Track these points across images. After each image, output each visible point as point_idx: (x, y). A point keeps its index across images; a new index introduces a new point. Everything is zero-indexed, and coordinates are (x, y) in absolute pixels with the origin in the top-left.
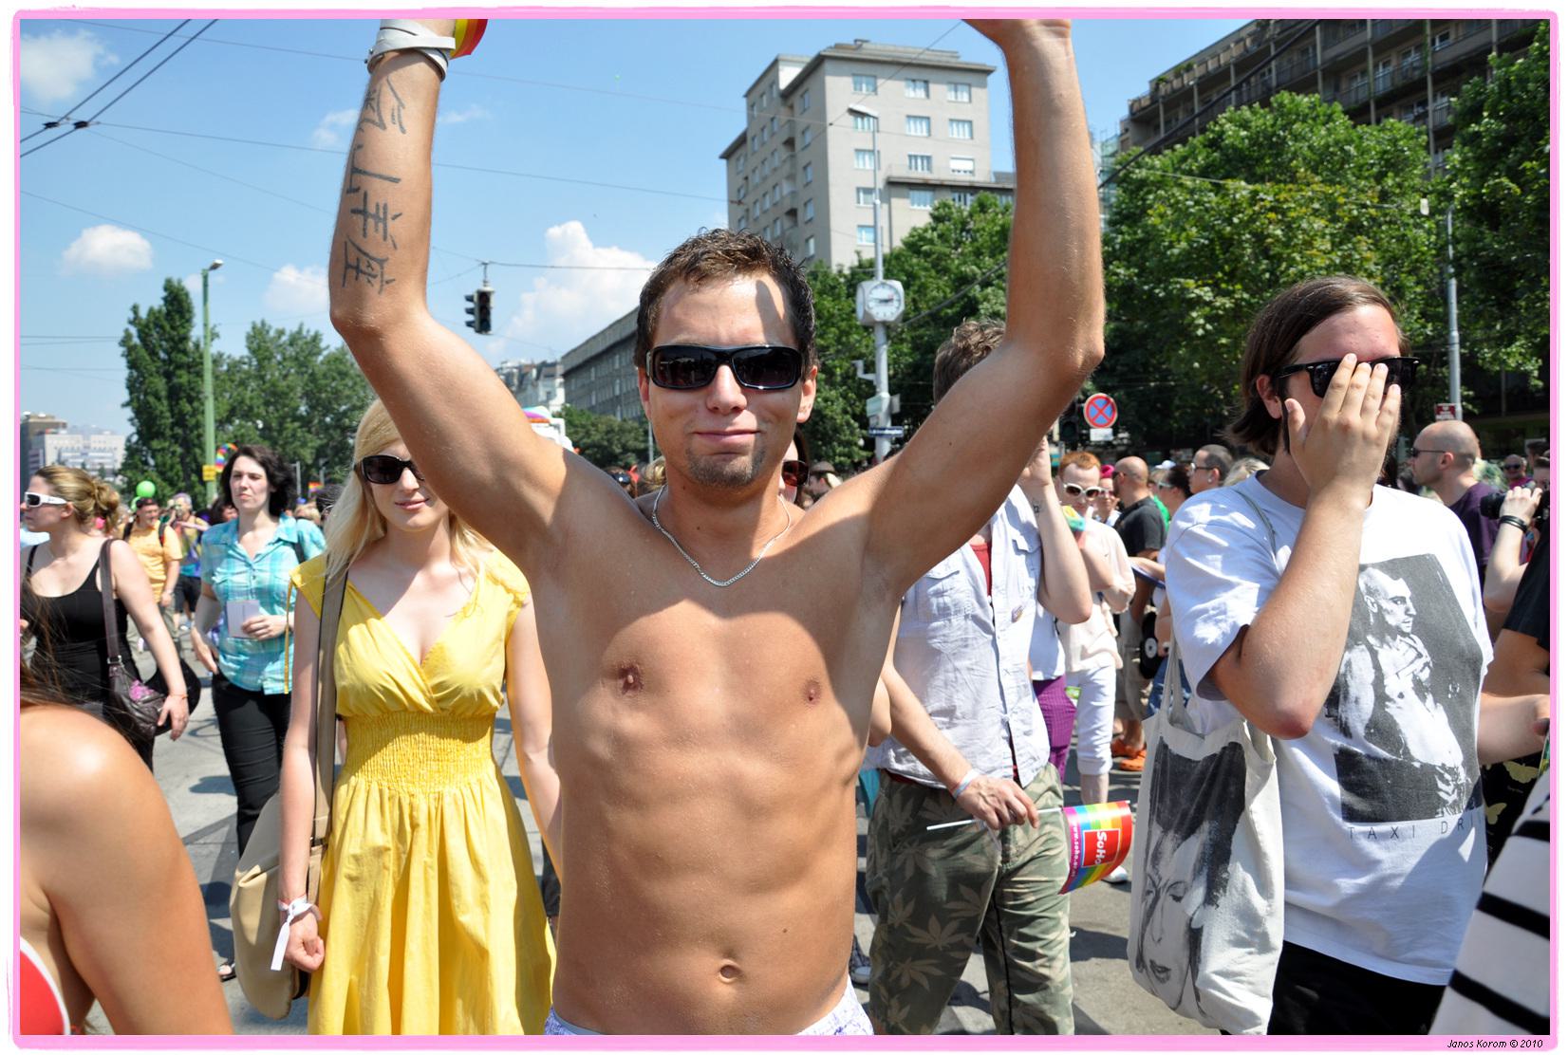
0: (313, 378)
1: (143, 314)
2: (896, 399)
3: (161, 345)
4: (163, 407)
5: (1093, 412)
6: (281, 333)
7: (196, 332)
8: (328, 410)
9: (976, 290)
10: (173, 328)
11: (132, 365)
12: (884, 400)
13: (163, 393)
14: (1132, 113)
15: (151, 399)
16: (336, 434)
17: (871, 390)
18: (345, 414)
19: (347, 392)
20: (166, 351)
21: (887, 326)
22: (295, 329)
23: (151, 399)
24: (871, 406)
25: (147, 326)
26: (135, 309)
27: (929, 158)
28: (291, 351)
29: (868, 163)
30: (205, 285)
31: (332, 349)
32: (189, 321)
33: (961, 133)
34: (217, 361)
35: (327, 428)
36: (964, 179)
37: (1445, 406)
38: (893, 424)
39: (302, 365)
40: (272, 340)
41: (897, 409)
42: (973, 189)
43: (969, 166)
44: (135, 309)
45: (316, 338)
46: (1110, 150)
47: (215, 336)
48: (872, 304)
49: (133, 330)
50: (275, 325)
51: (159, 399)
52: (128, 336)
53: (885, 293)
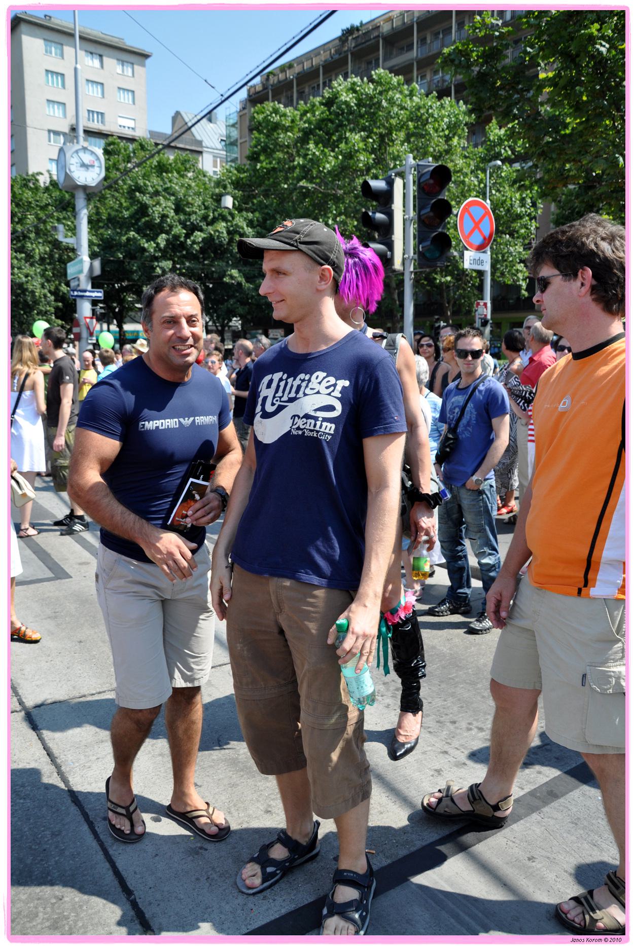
2: (97, 264)
5: (468, 225)
9: (146, 199)
12: (84, 265)
14: (249, 96)
17: (70, 252)
21: (85, 188)
24: (71, 269)
27: (102, 114)
29: (58, 111)
33: (127, 98)
36: (129, 133)
37: (482, 303)
38: (93, 287)
41: (97, 271)
42: (132, 140)
43: (131, 124)
46: (232, 122)
48: (73, 168)
53: (87, 158)
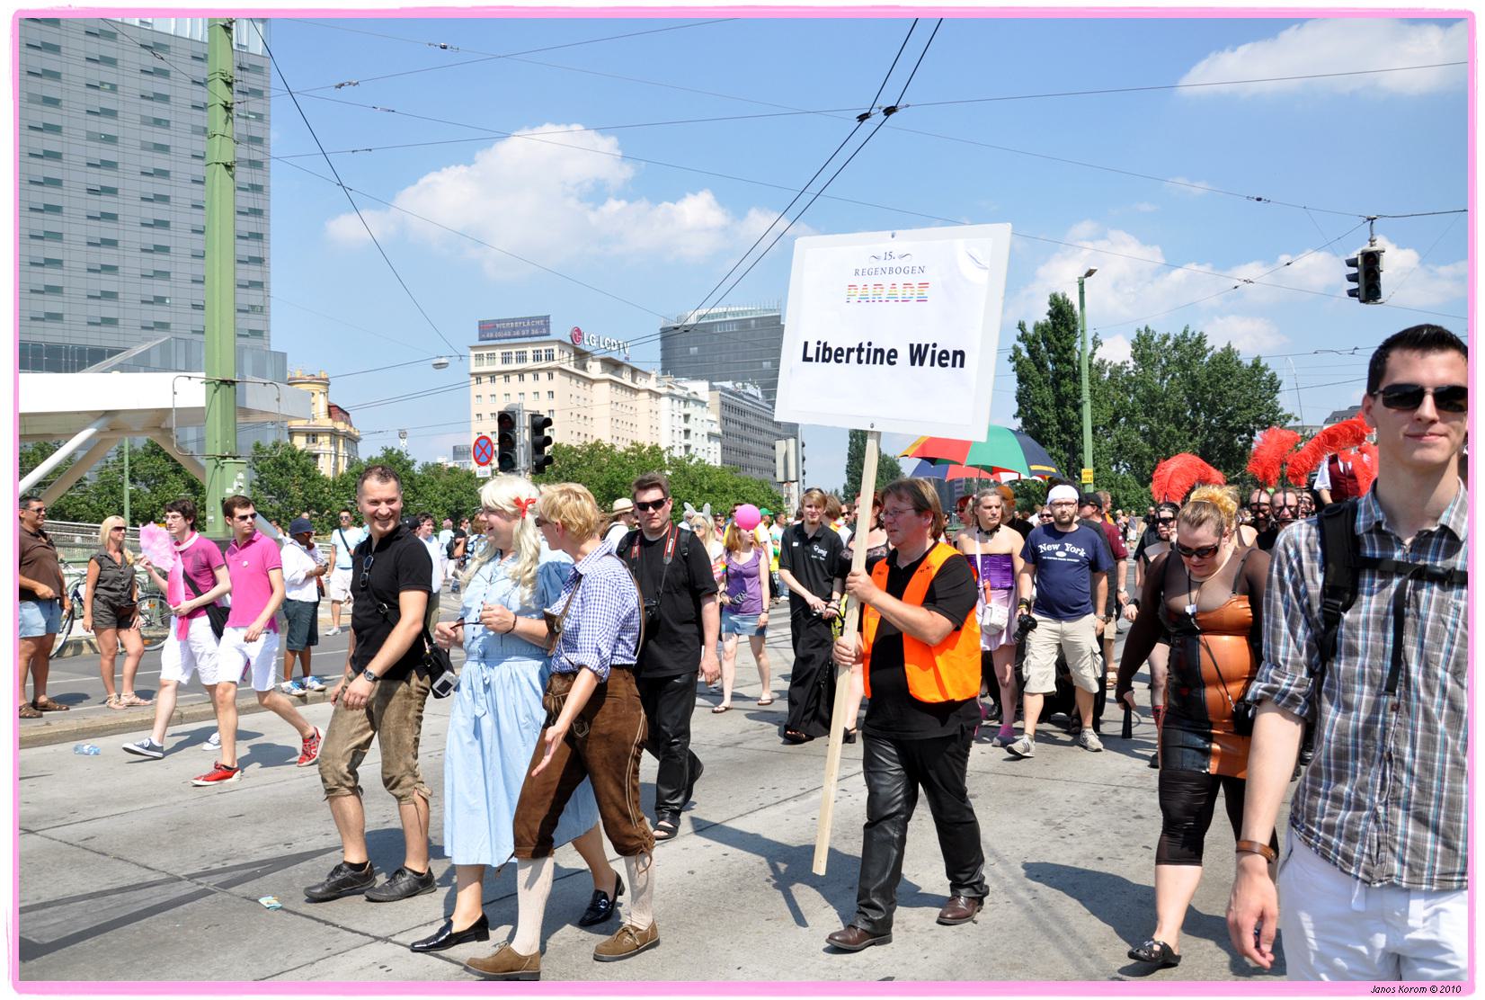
0: (1195, 383)
1: (1030, 330)
3: (1048, 358)
4: (1050, 415)
6: (1167, 337)
7: (1077, 345)
8: (1212, 411)
10: (1059, 340)
11: (1021, 380)
13: (1050, 401)
15: (1038, 410)
16: (1222, 435)
18: (1231, 416)
19: (1231, 393)
20: (1054, 362)
22: (1180, 332)
23: (1038, 410)
25: (1034, 340)
26: (1021, 326)
28: (1177, 354)
30: (1082, 293)
31: (1218, 350)
32: (1074, 331)
34: (1100, 368)
35: (1212, 430)
39: (1185, 368)
40: (1157, 347)
44: (1021, 326)
45: (1200, 340)
47: (1097, 343)
49: (1021, 345)
50: (1159, 330)
51: (1045, 408)
52: (1017, 351)
